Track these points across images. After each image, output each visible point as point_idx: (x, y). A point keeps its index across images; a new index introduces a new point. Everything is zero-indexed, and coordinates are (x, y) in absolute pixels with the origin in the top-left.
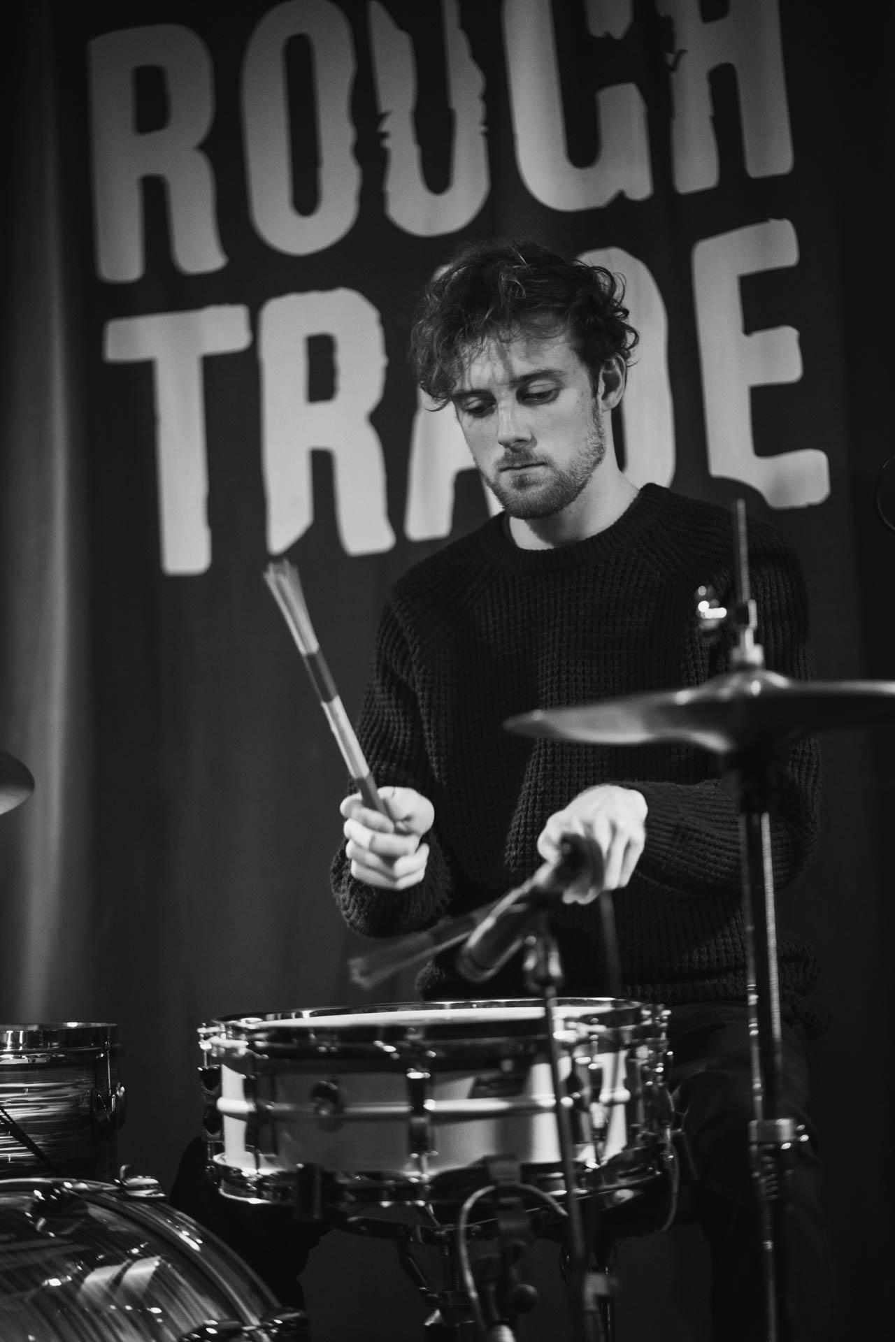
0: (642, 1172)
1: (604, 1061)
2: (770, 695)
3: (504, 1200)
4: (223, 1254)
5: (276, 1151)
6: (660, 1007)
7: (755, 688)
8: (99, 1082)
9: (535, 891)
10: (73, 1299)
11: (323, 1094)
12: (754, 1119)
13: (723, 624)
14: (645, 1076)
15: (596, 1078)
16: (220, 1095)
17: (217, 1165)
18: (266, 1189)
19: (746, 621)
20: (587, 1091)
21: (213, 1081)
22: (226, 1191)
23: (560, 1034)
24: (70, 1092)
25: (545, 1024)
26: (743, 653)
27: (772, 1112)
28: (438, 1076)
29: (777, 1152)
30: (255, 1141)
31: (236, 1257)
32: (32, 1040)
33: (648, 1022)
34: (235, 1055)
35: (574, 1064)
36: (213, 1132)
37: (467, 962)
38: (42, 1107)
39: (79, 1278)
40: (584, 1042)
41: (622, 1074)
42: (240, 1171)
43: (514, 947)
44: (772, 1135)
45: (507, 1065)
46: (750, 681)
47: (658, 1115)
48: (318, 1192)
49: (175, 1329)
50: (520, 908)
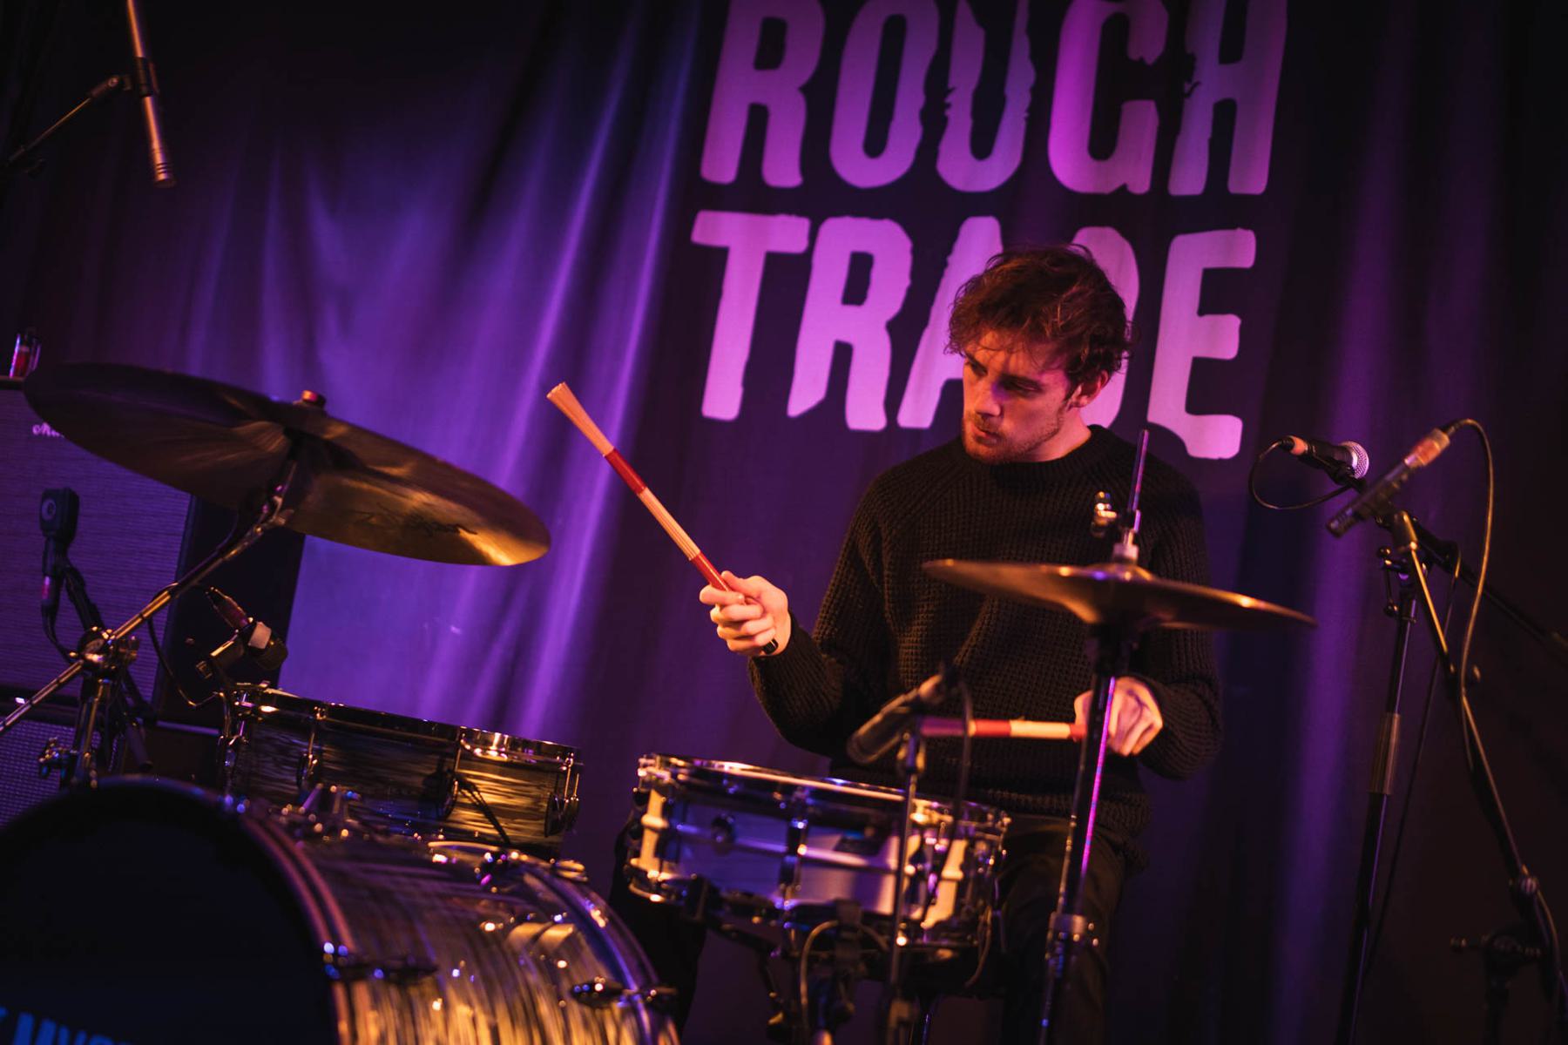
2: (1136, 584)
3: (845, 934)
4: (622, 934)
7: (1128, 576)
8: (558, 789)
10: (499, 944)
11: (720, 823)
13: (1112, 525)
14: (978, 864)
16: (645, 812)
17: (632, 866)
19: (1132, 526)
20: (928, 866)
21: (643, 800)
22: (636, 886)
23: (919, 817)
24: (535, 792)
26: (1124, 548)
27: (1069, 909)
30: (661, 852)
31: (632, 938)
35: (923, 841)
36: (634, 839)
37: (855, 745)
38: (510, 798)
39: (511, 927)
40: (934, 827)
42: (646, 873)
46: (1124, 571)
49: (571, 980)
50: (903, 710)
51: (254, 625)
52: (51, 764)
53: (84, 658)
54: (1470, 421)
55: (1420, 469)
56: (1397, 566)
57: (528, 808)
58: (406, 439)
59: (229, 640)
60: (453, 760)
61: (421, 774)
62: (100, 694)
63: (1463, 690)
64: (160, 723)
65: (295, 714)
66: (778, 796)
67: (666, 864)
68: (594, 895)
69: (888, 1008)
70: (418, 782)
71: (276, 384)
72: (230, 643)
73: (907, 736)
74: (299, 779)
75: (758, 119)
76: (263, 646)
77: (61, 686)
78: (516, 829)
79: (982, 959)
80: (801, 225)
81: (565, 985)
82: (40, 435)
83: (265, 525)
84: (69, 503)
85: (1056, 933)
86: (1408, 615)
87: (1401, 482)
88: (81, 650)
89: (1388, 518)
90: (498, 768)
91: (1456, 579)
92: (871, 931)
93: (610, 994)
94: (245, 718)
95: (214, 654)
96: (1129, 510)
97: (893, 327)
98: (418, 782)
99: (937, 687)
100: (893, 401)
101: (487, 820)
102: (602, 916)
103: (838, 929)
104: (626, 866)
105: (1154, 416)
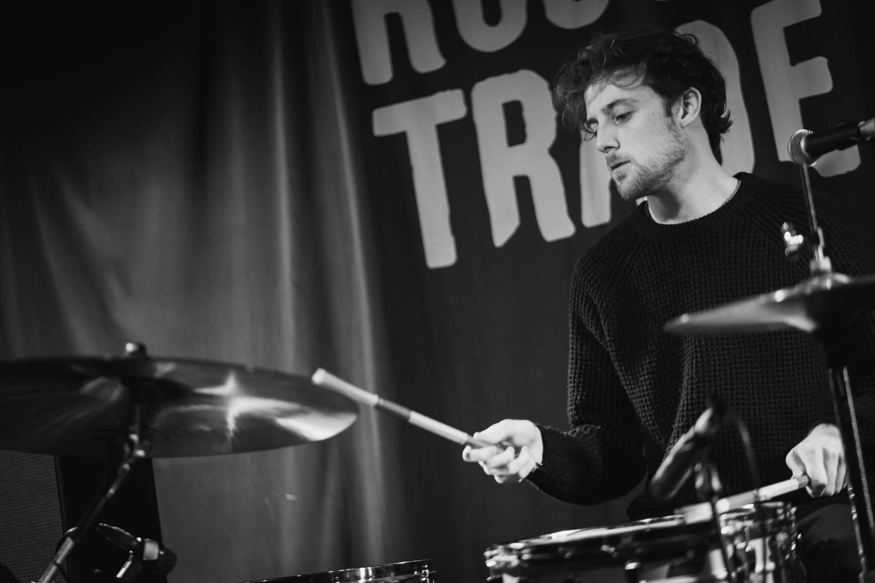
1: (756, 545)
2: (838, 288)
6: (789, 506)
7: (828, 284)
9: (697, 436)
12: (861, 571)
14: (784, 553)
15: (752, 555)
19: (818, 242)
20: (746, 566)
23: (726, 530)
25: (713, 523)
26: (818, 264)
33: (782, 517)
34: (509, 566)
35: (735, 548)
40: (741, 534)
41: (769, 553)
43: (687, 474)
50: (688, 447)
59: (127, 560)
66: (605, 548)
72: (128, 564)
73: (698, 467)
76: (155, 557)
80: (457, 95)
96: (811, 230)
97: (555, 151)
99: (711, 421)
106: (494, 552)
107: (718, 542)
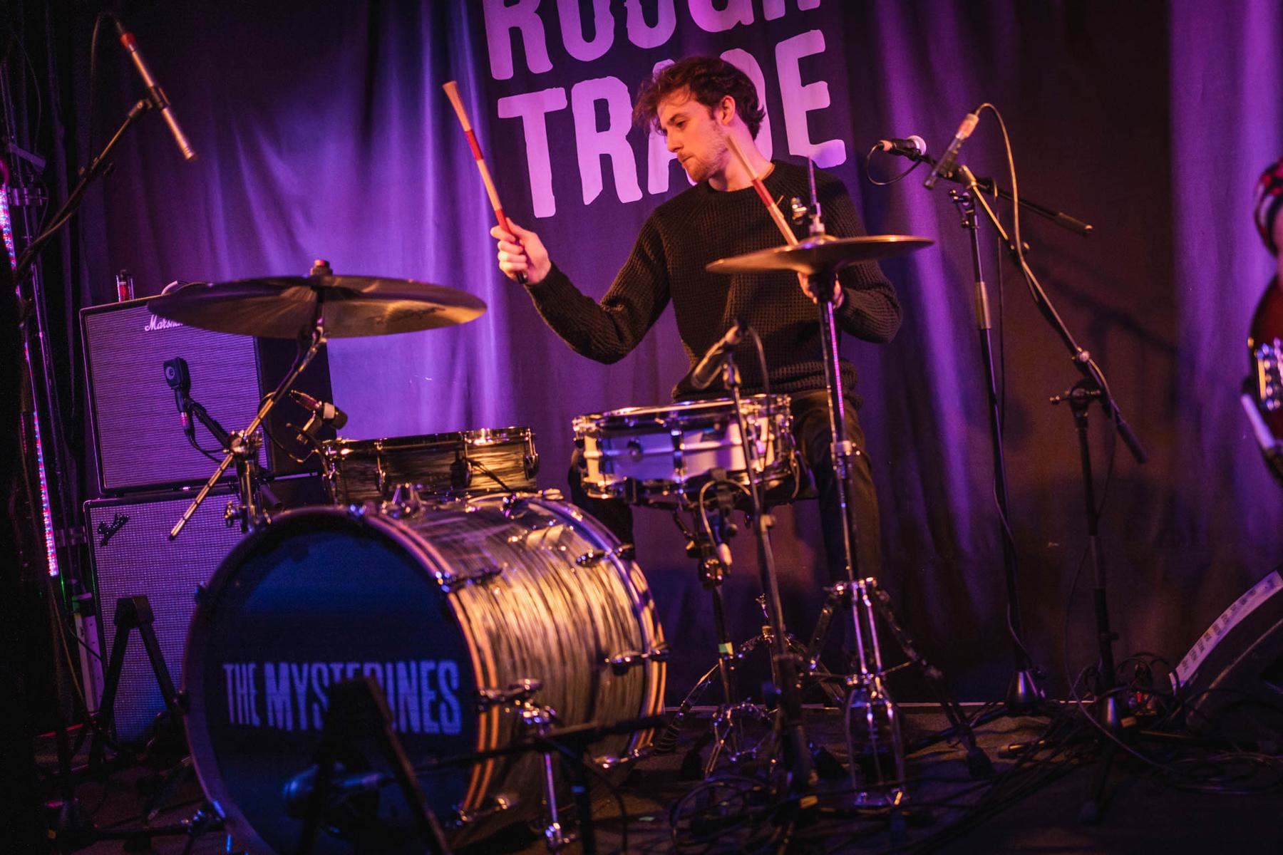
0: (782, 472)
2: (828, 246)
3: (720, 487)
4: (591, 521)
5: (612, 472)
7: (822, 242)
8: (527, 452)
9: (726, 343)
11: (632, 445)
14: (780, 428)
15: (758, 429)
16: (584, 450)
17: (586, 483)
18: (610, 491)
19: (816, 213)
20: (754, 436)
21: (581, 444)
22: (592, 493)
23: (743, 411)
24: (514, 457)
25: (735, 406)
26: (815, 227)
27: (840, 439)
28: (686, 433)
29: (844, 457)
30: (602, 469)
31: (600, 524)
32: (494, 433)
34: (590, 431)
35: (748, 424)
37: (696, 380)
38: (501, 464)
39: (526, 536)
40: (752, 414)
42: (597, 484)
43: (718, 371)
44: (841, 448)
45: (717, 426)
46: (819, 239)
47: (787, 448)
48: (634, 490)
49: (574, 555)
50: (720, 352)
51: (323, 405)
52: (232, 518)
53: (233, 451)
54: (986, 105)
55: (966, 139)
56: (962, 199)
57: (513, 467)
58: (371, 274)
59: (311, 417)
60: (463, 452)
61: (447, 465)
62: (248, 470)
63: (1022, 258)
64: (276, 479)
65: (363, 450)
67: (607, 476)
68: (570, 505)
69: (759, 523)
70: (447, 469)
71: (278, 265)
72: (312, 420)
73: (726, 366)
74: (378, 486)
75: (516, 36)
76: (332, 416)
77: (223, 471)
78: (511, 481)
79: (797, 480)
81: (572, 560)
82: (150, 331)
83: (317, 345)
84: (181, 366)
85: (836, 454)
86: (974, 225)
87: (958, 149)
88: (229, 446)
89: (956, 173)
90: (489, 449)
91: (997, 198)
92: (732, 481)
93: (598, 557)
94: (334, 460)
95: (306, 428)
97: (629, 138)
98: (447, 469)
99: (736, 334)
100: (643, 181)
101: (492, 480)
102: (578, 514)
103: (715, 485)
104: (582, 484)
105: (793, 151)
106: (580, 421)
107: (736, 418)
